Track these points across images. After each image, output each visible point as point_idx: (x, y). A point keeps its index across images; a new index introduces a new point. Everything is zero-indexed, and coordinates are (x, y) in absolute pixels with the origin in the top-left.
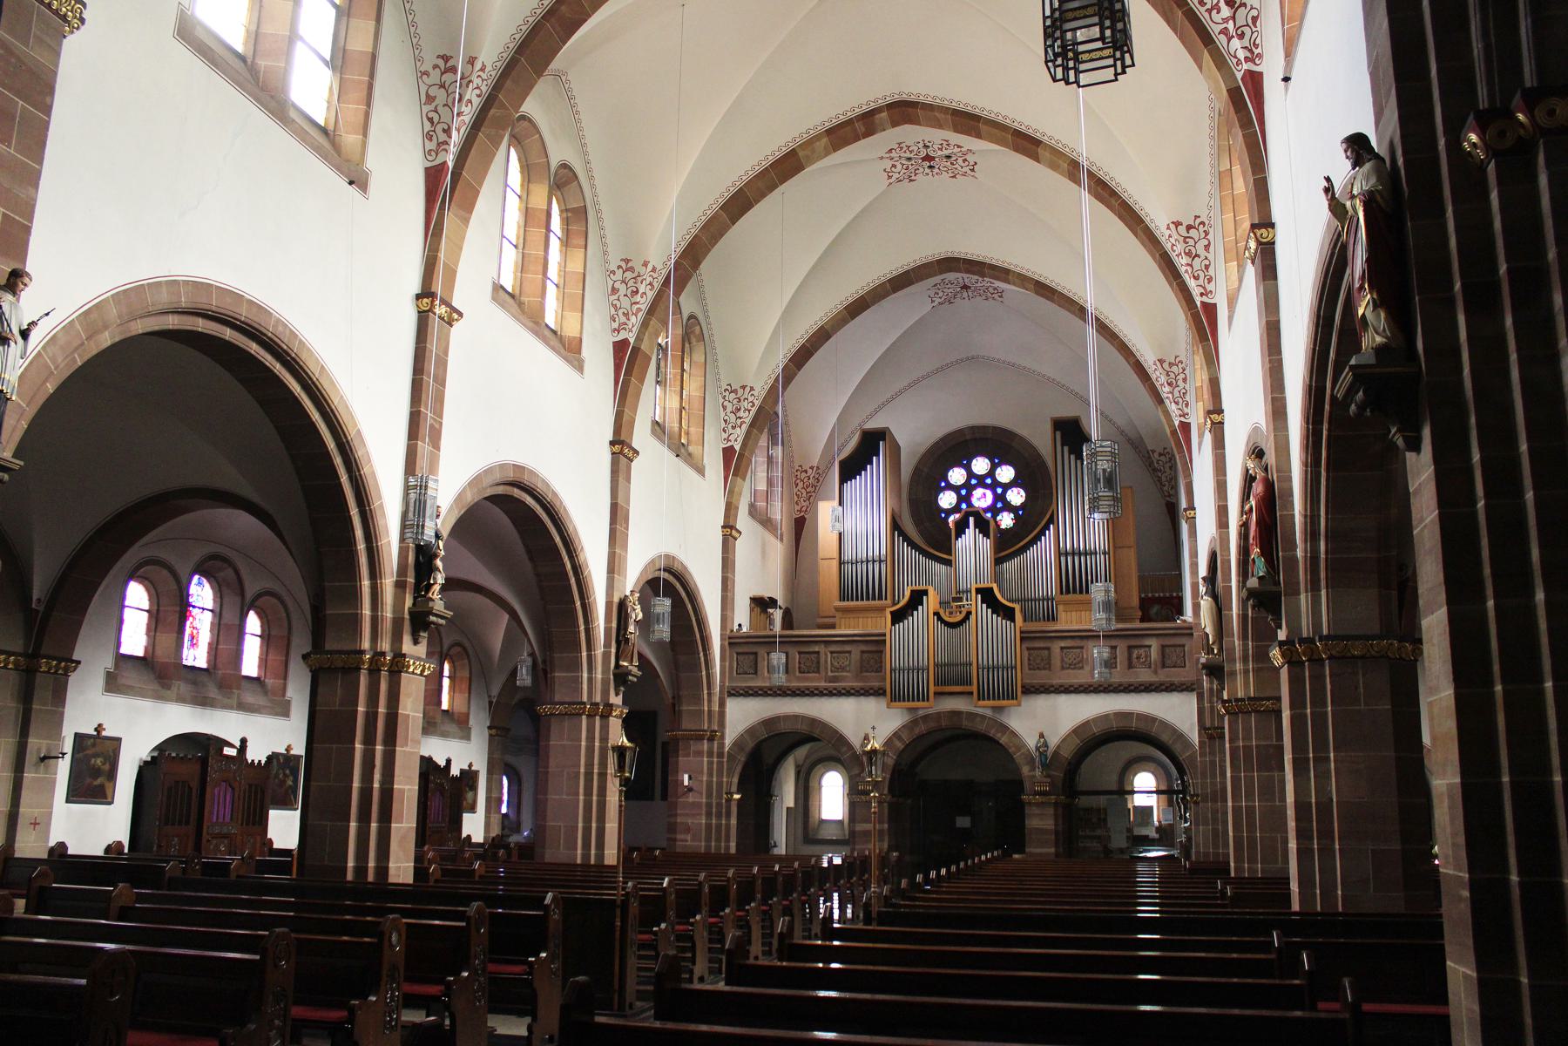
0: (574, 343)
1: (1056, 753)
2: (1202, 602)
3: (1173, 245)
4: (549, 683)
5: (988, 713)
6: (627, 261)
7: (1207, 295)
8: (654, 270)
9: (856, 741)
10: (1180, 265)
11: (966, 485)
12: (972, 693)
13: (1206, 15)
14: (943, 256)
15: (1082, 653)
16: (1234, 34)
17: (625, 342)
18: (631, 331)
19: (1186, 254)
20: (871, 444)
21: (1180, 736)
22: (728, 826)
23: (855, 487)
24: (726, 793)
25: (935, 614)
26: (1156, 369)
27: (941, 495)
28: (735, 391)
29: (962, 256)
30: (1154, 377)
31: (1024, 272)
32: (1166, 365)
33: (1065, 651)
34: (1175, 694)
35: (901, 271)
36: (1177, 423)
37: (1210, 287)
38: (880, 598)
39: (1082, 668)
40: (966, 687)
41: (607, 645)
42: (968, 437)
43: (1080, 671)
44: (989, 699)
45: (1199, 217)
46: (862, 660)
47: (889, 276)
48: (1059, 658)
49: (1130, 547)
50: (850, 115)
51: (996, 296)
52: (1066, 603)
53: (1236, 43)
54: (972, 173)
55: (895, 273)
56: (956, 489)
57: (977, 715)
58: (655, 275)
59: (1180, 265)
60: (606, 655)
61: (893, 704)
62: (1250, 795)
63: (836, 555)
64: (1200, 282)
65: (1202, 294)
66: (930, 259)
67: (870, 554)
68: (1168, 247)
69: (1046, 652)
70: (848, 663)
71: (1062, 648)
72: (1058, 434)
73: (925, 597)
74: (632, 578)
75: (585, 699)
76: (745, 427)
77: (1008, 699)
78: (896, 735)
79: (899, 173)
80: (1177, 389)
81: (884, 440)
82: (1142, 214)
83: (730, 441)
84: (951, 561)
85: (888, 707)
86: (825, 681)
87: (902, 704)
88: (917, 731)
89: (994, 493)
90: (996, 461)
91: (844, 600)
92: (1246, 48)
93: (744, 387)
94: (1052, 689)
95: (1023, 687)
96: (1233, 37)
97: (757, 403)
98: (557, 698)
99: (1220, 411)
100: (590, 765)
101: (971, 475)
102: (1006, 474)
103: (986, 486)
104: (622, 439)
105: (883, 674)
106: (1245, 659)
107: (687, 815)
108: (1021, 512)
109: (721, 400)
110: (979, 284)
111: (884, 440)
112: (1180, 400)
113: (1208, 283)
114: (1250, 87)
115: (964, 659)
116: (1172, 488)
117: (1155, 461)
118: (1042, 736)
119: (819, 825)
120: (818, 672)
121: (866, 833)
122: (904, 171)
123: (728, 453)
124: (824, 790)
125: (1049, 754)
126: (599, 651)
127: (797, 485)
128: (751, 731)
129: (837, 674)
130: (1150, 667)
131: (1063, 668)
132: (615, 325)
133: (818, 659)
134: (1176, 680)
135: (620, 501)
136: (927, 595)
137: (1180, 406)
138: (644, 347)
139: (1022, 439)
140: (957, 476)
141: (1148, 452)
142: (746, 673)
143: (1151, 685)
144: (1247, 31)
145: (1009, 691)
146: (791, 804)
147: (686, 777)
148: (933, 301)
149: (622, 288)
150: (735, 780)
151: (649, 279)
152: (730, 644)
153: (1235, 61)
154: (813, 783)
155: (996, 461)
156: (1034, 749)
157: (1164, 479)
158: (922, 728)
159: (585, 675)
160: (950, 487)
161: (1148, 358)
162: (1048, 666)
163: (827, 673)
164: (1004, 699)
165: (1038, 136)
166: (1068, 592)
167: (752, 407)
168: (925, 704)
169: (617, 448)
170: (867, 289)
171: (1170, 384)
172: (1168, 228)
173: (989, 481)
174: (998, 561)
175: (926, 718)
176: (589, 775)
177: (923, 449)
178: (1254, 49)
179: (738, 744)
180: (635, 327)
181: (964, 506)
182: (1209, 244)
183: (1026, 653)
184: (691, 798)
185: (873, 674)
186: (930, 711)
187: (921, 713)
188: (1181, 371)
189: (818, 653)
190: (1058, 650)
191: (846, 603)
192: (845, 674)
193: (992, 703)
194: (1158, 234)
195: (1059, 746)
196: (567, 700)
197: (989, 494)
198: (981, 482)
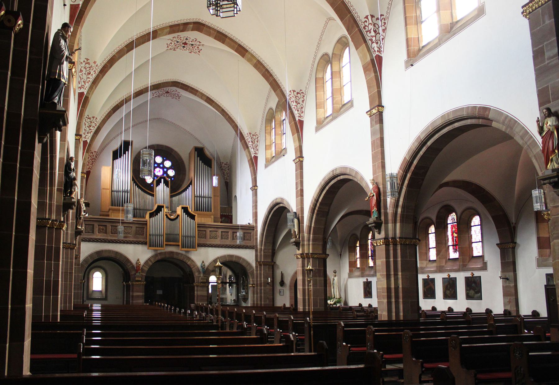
1: (207, 268)
3: (291, 98)
5: (184, 253)
6: (88, 60)
8: (97, 66)
10: (292, 105)
13: (365, 33)
15: (217, 233)
16: (375, 42)
18: (85, 89)
19: (295, 102)
20: (126, 145)
21: (249, 264)
23: (118, 162)
28: (90, 118)
30: (246, 139)
32: (251, 135)
33: (211, 232)
34: (248, 249)
35: (157, 83)
36: (253, 156)
37: (302, 115)
39: (217, 238)
43: (216, 240)
44: (185, 248)
45: (302, 90)
46: (136, 230)
48: (209, 236)
49: (218, 196)
50: (179, 22)
53: (374, 45)
54: (199, 53)
57: (179, 253)
58: (97, 68)
59: (292, 105)
61: (150, 248)
65: (299, 117)
69: (204, 232)
71: (210, 231)
72: (196, 152)
73: (163, 209)
76: (92, 133)
77: (192, 248)
78: (149, 259)
79: (172, 46)
80: (254, 144)
82: (280, 85)
83: (86, 138)
84: (154, 195)
88: (157, 259)
89: (163, 170)
90: (165, 159)
92: (378, 47)
93: (93, 117)
94: (207, 245)
96: (374, 42)
97: (98, 125)
99: (303, 157)
102: (168, 164)
103: (161, 168)
106: (309, 240)
108: (173, 179)
110: (174, 92)
112: (255, 148)
113: (302, 113)
114: (378, 60)
115: (176, 232)
116: (228, 176)
118: (203, 262)
122: (174, 46)
125: (205, 269)
127: (88, 158)
129: (126, 235)
131: (210, 238)
132: (80, 86)
134: (249, 245)
137: (255, 150)
139: (176, 152)
141: (221, 163)
142: (89, 232)
144: (379, 42)
145: (193, 247)
149: (84, 70)
151: (95, 69)
153: (373, 50)
155: (165, 159)
156: (200, 267)
157: (225, 173)
158: (159, 257)
161: (245, 132)
164: (191, 248)
165: (247, 48)
167: (95, 126)
168: (162, 248)
171: (252, 142)
172: (290, 91)
173: (161, 166)
174: (172, 196)
175: (161, 253)
178: (380, 49)
180: (87, 88)
182: (304, 100)
187: (159, 252)
191: (113, 207)
192: (129, 235)
193: (185, 249)
194: (285, 93)
197: (161, 170)
198: (159, 165)
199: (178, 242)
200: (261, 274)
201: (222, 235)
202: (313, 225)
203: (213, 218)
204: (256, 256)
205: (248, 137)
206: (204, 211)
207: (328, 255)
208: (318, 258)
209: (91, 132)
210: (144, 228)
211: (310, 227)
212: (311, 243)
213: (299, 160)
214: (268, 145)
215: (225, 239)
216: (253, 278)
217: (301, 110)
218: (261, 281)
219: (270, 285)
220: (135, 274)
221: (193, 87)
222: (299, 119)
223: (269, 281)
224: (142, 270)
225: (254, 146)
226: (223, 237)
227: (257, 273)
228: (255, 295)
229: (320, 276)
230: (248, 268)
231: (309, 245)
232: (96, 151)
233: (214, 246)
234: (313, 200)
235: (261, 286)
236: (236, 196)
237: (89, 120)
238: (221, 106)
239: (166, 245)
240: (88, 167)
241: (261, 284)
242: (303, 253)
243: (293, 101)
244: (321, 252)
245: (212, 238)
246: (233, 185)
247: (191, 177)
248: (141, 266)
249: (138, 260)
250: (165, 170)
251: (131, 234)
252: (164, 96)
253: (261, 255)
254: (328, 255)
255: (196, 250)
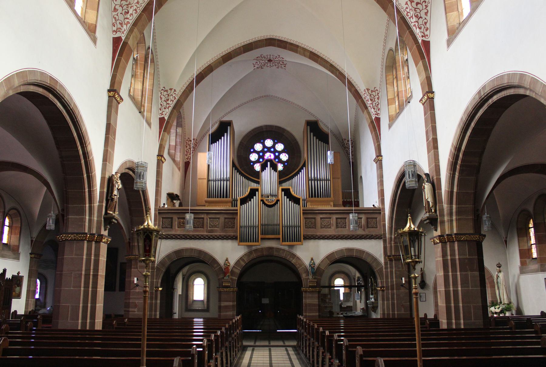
0: (91, 27)
1: (318, 268)
2: (426, 186)
3: (408, 12)
4: (65, 222)
5: (286, 248)
7: (425, 37)
9: (221, 262)
10: (411, 23)
11: (263, 151)
12: (279, 239)
14: (268, 37)
15: (331, 220)
17: (119, 38)
18: (123, 33)
19: (415, 16)
21: (375, 260)
22: (156, 303)
24: (156, 287)
25: (261, 200)
26: (365, 93)
27: (251, 155)
28: (167, 91)
29: (277, 38)
30: (363, 97)
31: (305, 47)
33: (322, 219)
35: (248, 42)
36: (373, 118)
37: (426, 33)
38: (226, 197)
39: (330, 228)
40: (276, 236)
41: (101, 201)
42: (264, 130)
43: (330, 229)
44: (287, 241)
46: (225, 222)
47: (243, 44)
49: (339, 178)
51: (283, 66)
52: (311, 202)
55: (246, 43)
56: (258, 153)
57: (281, 249)
58: (138, 6)
59: (411, 23)
60: (100, 207)
61: (241, 243)
62: (455, 284)
63: (206, 177)
64: (422, 30)
65: (422, 36)
66: (262, 38)
67: (222, 176)
68: (405, 14)
69: (314, 220)
70: (218, 223)
71: (321, 218)
72: (309, 127)
73: (257, 192)
74: (116, 167)
75: (87, 231)
76: (170, 109)
77: (297, 241)
78: (241, 258)
80: (374, 102)
81: (230, 126)
83: (163, 115)
84: (259, 182)
85: (239, 245)
86: (207, 232)
87: (245, 243)
88: (252, 257)
89: (275, 155)
90: (276, 141)
91: (209, 198)
93: (171, 89)
94: (317, 237)
95: (304, 236)
97: (177, 98)
98: (70, 230)
99: (433, 92)
100: (88, 270)
101: (264, 146)
102: (280, 147)
103: (271, 152)
104: (115, 88)
105: (235, 229)
106: (451, 214)
107: (135, 298)
108: (286, 164)
109: (160, 95)
110: (277, 59)
111: (230, 126)
112: (376, 107)
113: (426, 31)
115: (276, 222)
117: (345, 144)
118: (312, 259)
119: (192, 303)
120: (203, 227)
121: (226, 307)
123: (162, 120)
124: (195, 286)
125: (315, 268)
126: (96, 204)
127: (187, 147)
128: (168, 256)
129: (212, 229)
130: (361, 228)
131: (321, 228)
132: (115, 29)
133: (203, 221)
134: (374, 234)
135: (112, 122)
136: (258, 191)
137: (376, 110)
138: (130, 42)
139: (288, 132)
140: (258, 147)
141: (343, 140)
143: (363, 236)
146: (180, 293)
147: (136, 279)
148: (254, 66)
150: (160, 281)
151: (135, 7)
152: (159, 213)
154: (190, 283)
155: (276, 141)
156: (308, 266)
158: (254, 255)
159: (87, 218)
160: (255, 151)
161: (361, 87)
162: (314, 226)
163: (208, 228)
164: (295, 241)
166: (312, 197)
167: (174, 99)
168: (257, 243)
169: (112, 94)
170: (232, 49)
171: (371, 100)
173: (272, 150)
175: (256, 250)
176: (87, 276)
177: (244, 134)
179: (162, 263)
181: (261, 160)
183: (304, 220)
184: (138, 290)
185: (231, 229)
186: (258, 247)
187: (254, 248)
188: (377, 94)
189: (203, 218)
190: (319, 219)
191: (210, 199)
195: (319, 265)
196: (76, 231)
199: (279, 234)
200: (391, 272)
201: (337, 223)
202: (455, 190)
203: (332, 205)
204: (385, 248)
205: (366, 95)
206: (321, 197)
207: (485, 236)
208: (466, 240)
209: (169, 107)
210: (235, 218)
211: (450, 193)
212: (454, 218)
213: (428, 98)
214: (391, 99)
215: (341, 227)
216: (382, 278)
217: (425, 26)
218: (392, 281)
219: (405, 287)
220: (223, 278)
221: (292, 42)
222: (423, 40)
223: (404, 282)
224: (232, 273)
225: (374, 105)
226: (339, 225)
227: (387, 272)
228: (386, 302)
229: (472, 270)
230: (374, 265)
231: (451, 221)
232: (195, 138)
233: (326, 237)
234: (453, 150)
235: (392, 289)
236: (361, 177)
237: (165, 93)
238: (329, 60)
239: (262, 239)
240: (187, 157)
241: (392, 286)
242: (442, 234)
243: (412, 17)
244: (471, 231)
245: (324, 228)
246: (358, 164)
247: (305, 158)
248: (230, 268)
249: (227, 260)
250: (266, 150)
251: (218, 228)
252: (268, 66)
253: (391, 246)
254: (485, 236)
255: (302, 245)
